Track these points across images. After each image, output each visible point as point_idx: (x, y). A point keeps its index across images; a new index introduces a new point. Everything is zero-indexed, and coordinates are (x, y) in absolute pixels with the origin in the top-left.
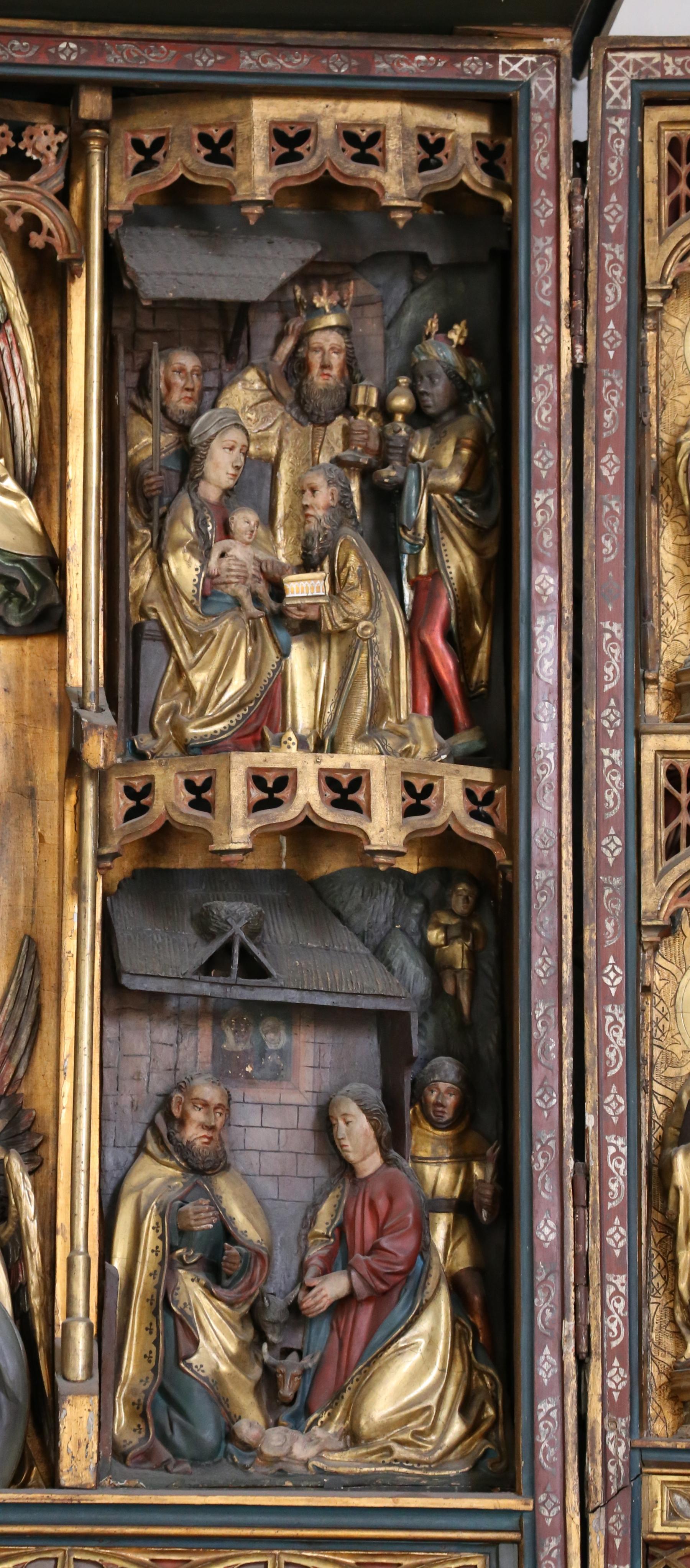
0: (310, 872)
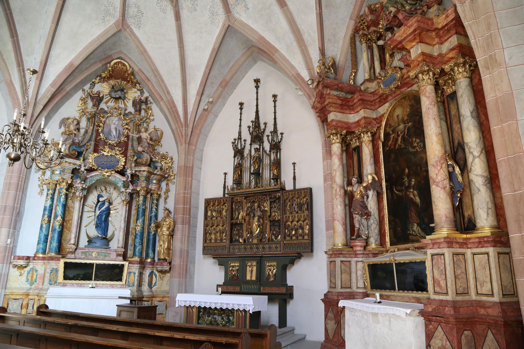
0: (274, 220)
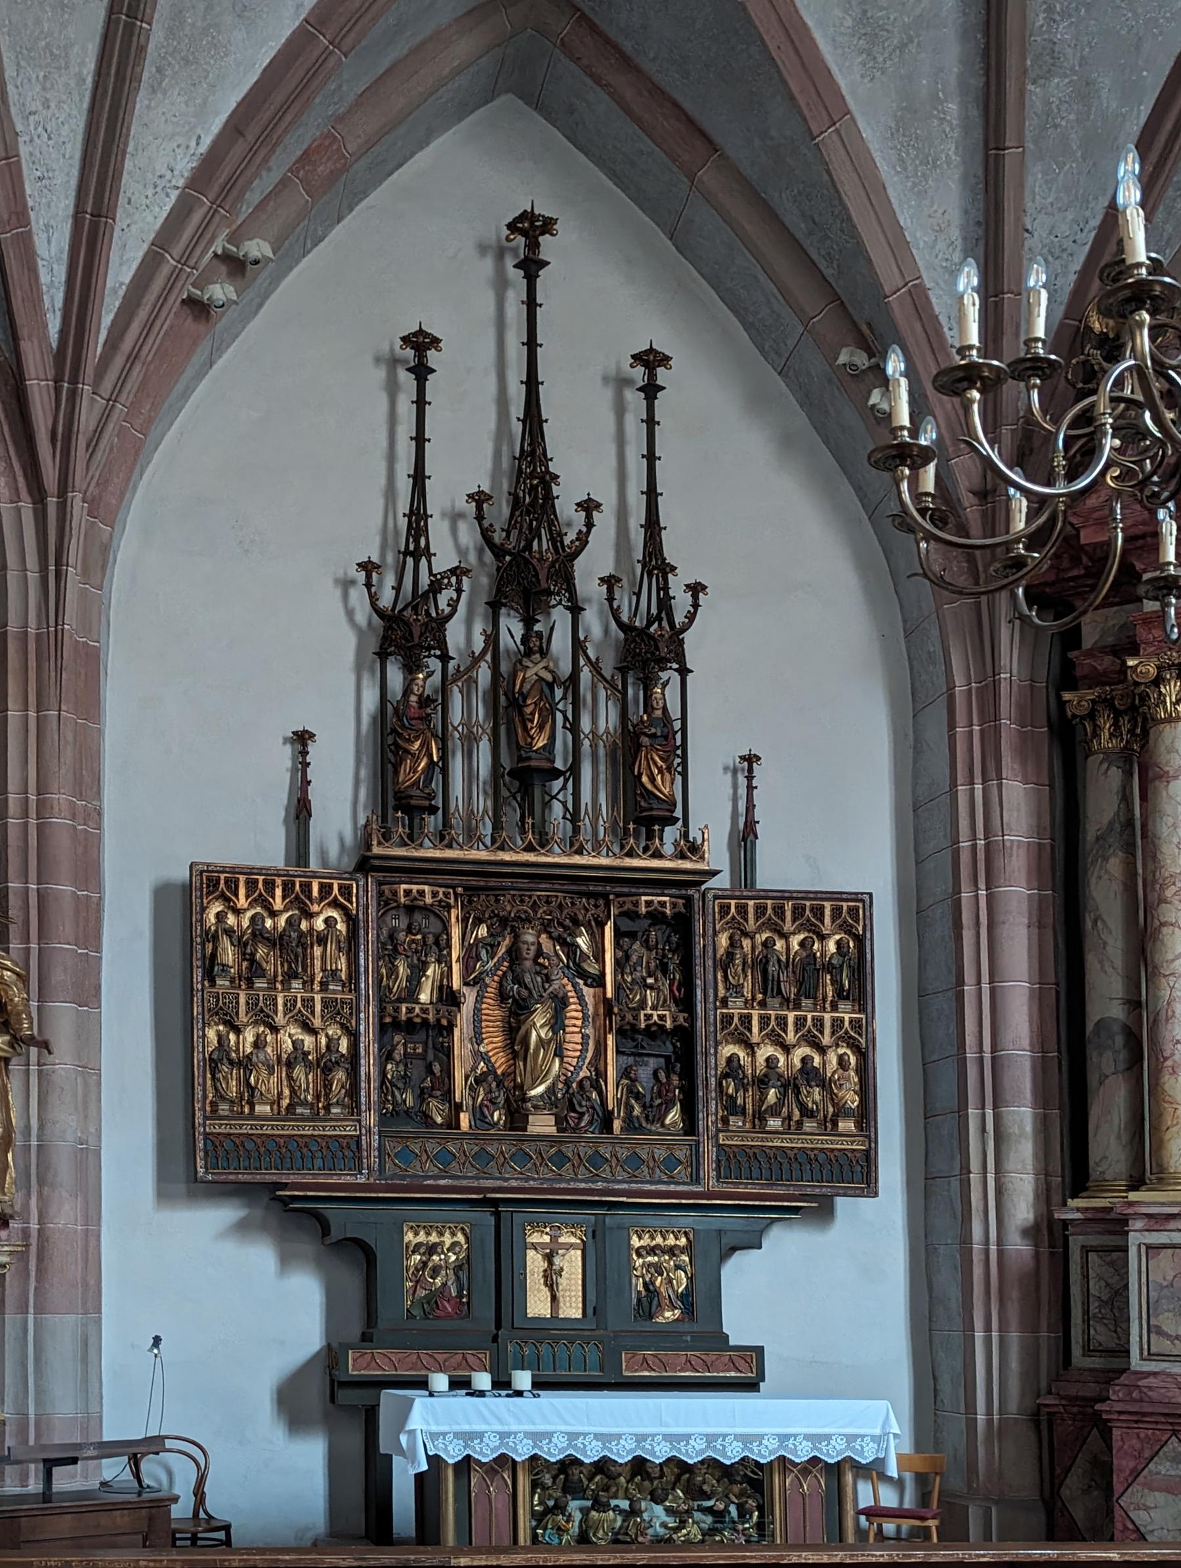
0: (655, 1032)
